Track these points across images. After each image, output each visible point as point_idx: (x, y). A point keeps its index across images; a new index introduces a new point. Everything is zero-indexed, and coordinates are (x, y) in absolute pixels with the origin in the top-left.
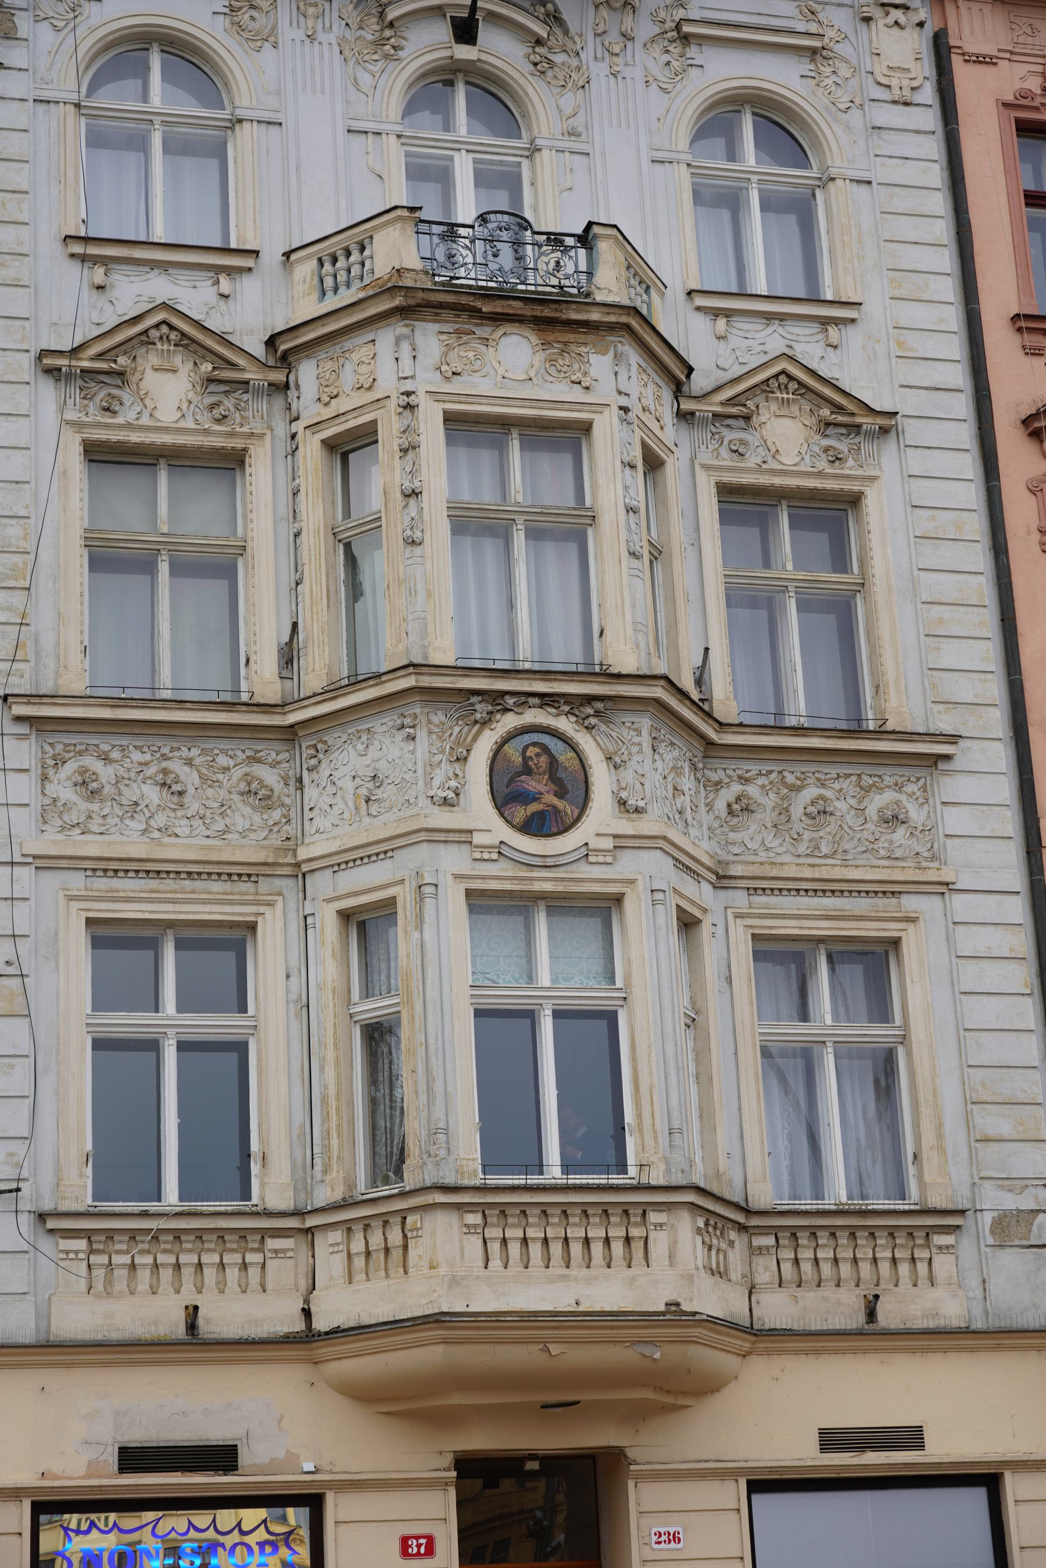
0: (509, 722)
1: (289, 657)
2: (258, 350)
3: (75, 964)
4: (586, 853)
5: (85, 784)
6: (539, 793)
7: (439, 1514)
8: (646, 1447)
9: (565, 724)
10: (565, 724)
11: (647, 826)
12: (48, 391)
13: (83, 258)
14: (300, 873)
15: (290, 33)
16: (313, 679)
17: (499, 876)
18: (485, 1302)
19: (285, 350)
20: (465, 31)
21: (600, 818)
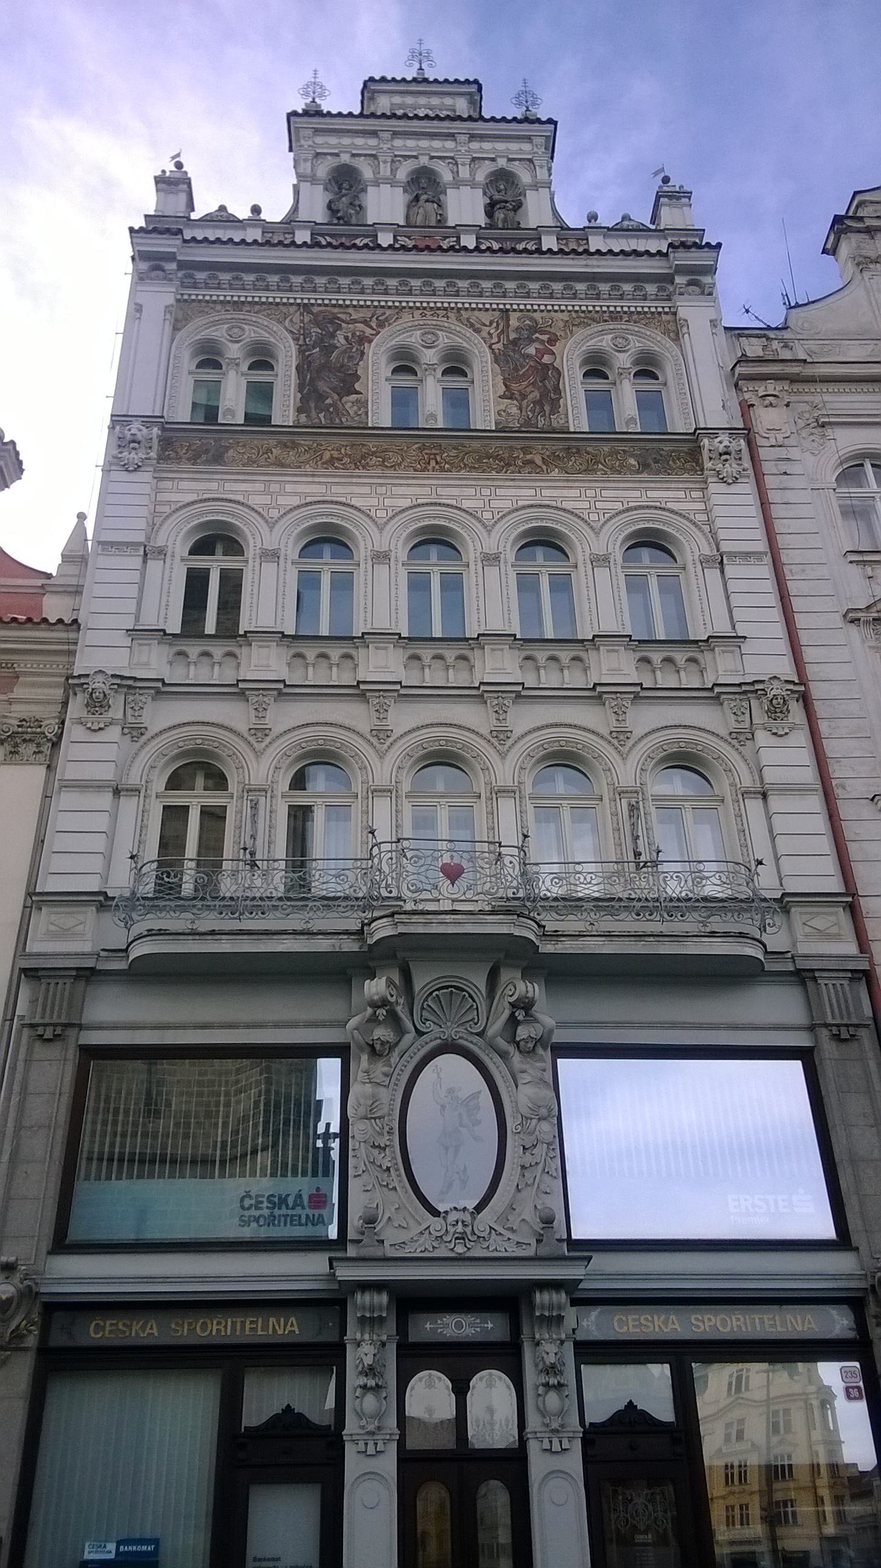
12: (853, 630)
13: (858, 562)
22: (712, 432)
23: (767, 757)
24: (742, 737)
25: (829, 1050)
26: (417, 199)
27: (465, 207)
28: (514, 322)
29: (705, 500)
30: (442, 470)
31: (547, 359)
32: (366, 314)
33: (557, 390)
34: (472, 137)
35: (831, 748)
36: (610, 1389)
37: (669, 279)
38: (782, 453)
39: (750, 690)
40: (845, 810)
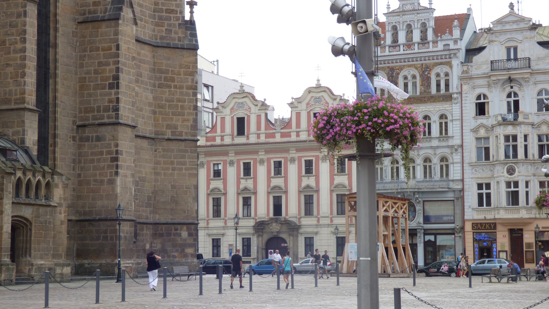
0: (508, 165)
1: (493, 157)
2: (490, 126)
3: (476, 187)
4: (515, 177)
5: (476, 171)
6: (511, 171)
7: (507, 234)
8: (525, 228)
9: (513, 165)
10: (513, 165)
11: (521, 174)
12: (472, 133)
14: (494, 178)
15: (494, 91)
16: (495, 160)
17: (507, 180)
18: (505, 217)
19: (493, 127)
20: (512, 87)
21: (516, 174)
22: (454, 93)
23: (454, 157)
24: (452, 153)
25: (455, 200)
26: (408, 32)
27: (417, 36)
28: (424, 66)
29: (452, 107)
30: (411, 104)
31: (429, 75)
32: (398, 67)
33: (430, 83)
34: (418, 14)
35: (464, 154)
36: (428, 238)
37: (450, 54)
38: (466, 95)
39: (452, 147)
40: (464, 165)
